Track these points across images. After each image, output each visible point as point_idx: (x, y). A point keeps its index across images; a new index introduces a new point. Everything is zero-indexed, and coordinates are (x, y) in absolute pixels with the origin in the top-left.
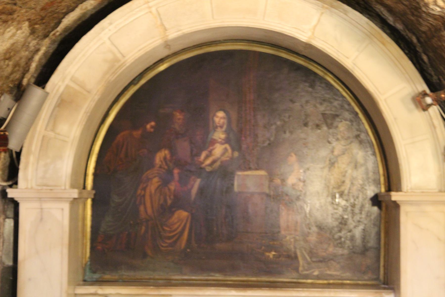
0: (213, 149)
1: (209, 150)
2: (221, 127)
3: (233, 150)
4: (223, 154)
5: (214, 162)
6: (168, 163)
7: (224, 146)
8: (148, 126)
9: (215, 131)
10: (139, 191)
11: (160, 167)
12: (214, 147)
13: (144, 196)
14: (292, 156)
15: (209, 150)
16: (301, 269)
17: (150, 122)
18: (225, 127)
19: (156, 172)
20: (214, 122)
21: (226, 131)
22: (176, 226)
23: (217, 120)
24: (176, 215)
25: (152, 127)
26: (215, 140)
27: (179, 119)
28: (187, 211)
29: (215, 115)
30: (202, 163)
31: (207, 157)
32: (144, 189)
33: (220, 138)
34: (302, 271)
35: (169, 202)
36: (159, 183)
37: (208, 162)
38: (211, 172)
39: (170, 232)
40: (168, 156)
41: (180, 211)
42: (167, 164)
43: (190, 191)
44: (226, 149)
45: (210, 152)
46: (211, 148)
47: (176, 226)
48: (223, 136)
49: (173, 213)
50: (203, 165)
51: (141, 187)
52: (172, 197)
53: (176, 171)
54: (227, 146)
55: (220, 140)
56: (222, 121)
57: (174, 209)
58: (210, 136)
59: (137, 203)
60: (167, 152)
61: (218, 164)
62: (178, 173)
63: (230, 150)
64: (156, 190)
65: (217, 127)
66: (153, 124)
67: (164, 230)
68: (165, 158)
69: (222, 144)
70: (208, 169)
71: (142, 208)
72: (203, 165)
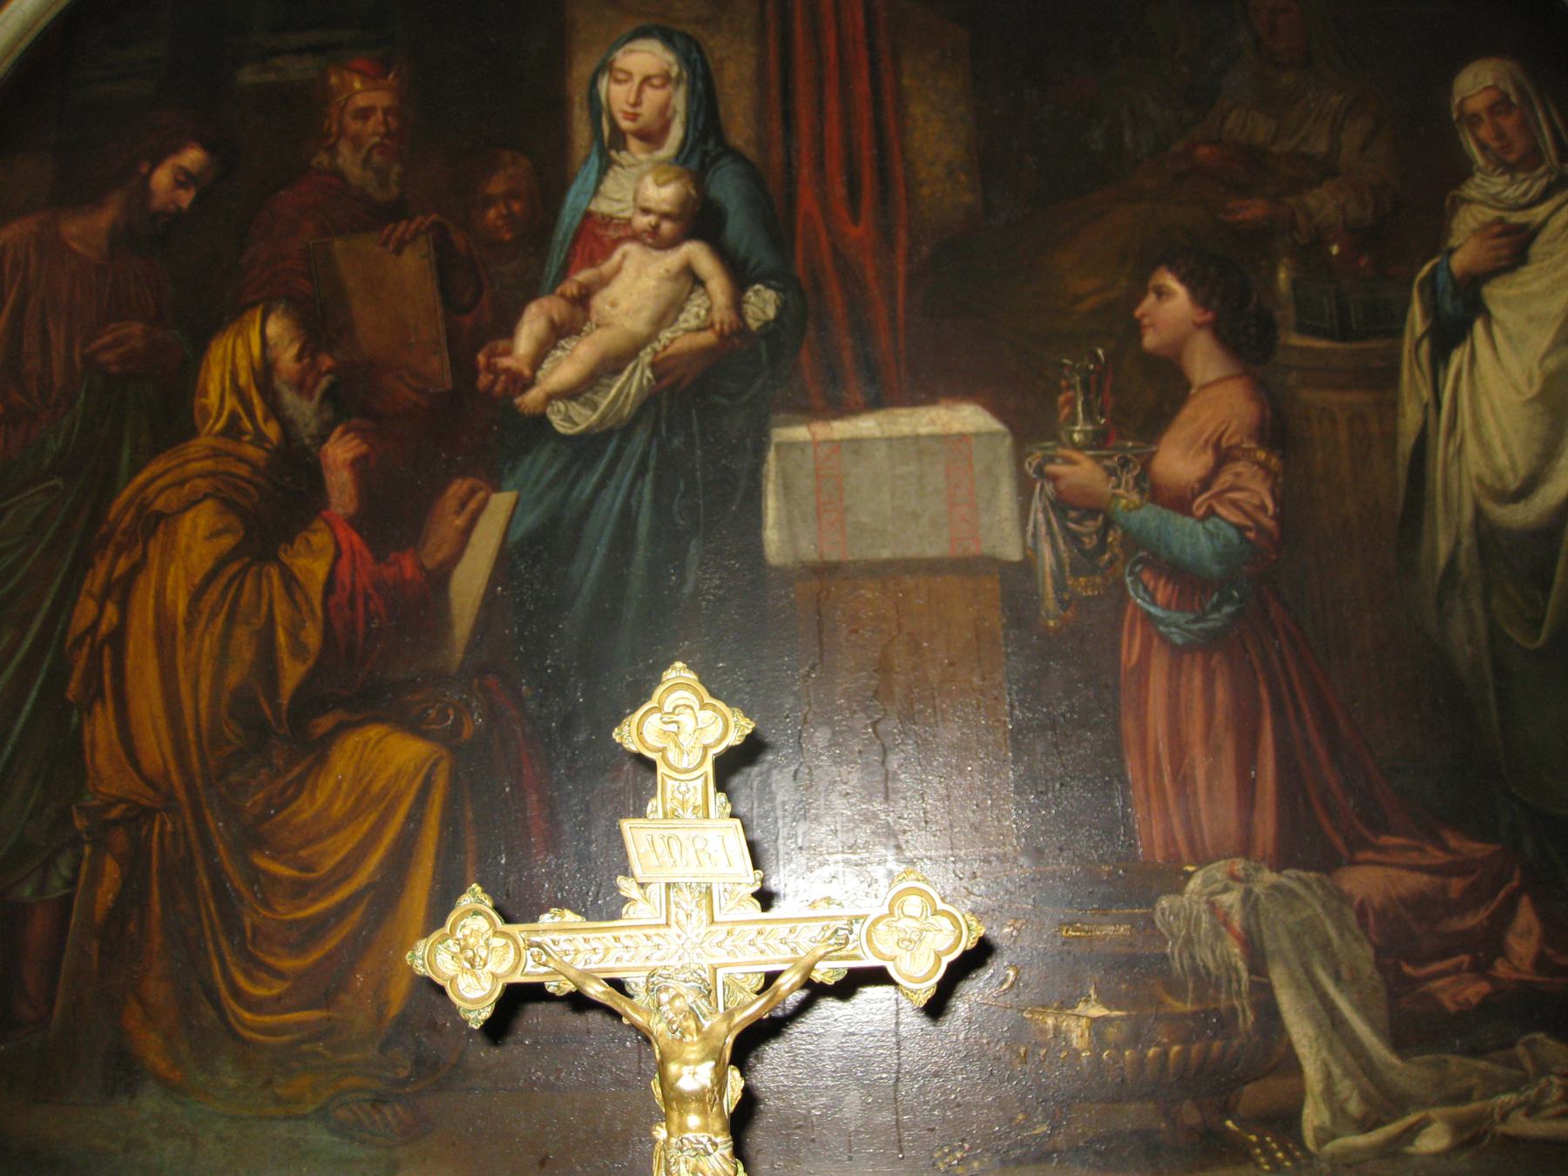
0: (604, 282)
1: (570, 288)
2: (652, 137)
3: (740, 276)
4: (668, 313)
5: (611, 365)
6: (289, 397)
7: (672, 260)
8: (162, 178)
9: (606, 165)
10: (86, 609)
11: (233, 429)
12: (607, 267)
13: (118, 637)
14: (1162, 293)
15: (570, 288)
16: (1314, 1116)
17: (176, 150)
18: (676, 132)
19: (209, 464)
20: (596, 107)
21: (682, 156)
22: (340, 847)
23: (617, 95)
24: (344, 760)
25: (184, 179)
26: (607, 221)
27: (364, 114)
28: (416, 728)
29: (606, 66)
30: (525, 383)
31: (559, 333)
32: (121, 591)
33: (646, 211)
34: (1325, 1136)
35: (292, 673)
36: (227, 542)
37: (564, 369)
38: (587, 446)
39: (301, 891)
40: (288, 357)
41: (373, 732)
42: (274, 408)
43: (440, 579)
44: (691, 278)
45: (582, 300)
46: (584, 275)
47: (340, 847)
48: (663, 194)
49: (318, 752)
50: (531, 398)
51: (96, 579)
52: (312, 636)
53: (340, 452)
54: (696, 253)
55: (643, 221)
56: (653, 97)
57: (325, 723)
58: (575, 201)
59: (74, 687)
60: (274, 328)
61: (635, 379)
62: (357, 465)
63: (718, 284)
64: (196, 596)
65: (619, 139)
66: (192, 157)
67: (255, 875)
68: (265, 372)
69: (657, 241)
70: (570, 420)
71: (101, 729)
72: (531, 398)
